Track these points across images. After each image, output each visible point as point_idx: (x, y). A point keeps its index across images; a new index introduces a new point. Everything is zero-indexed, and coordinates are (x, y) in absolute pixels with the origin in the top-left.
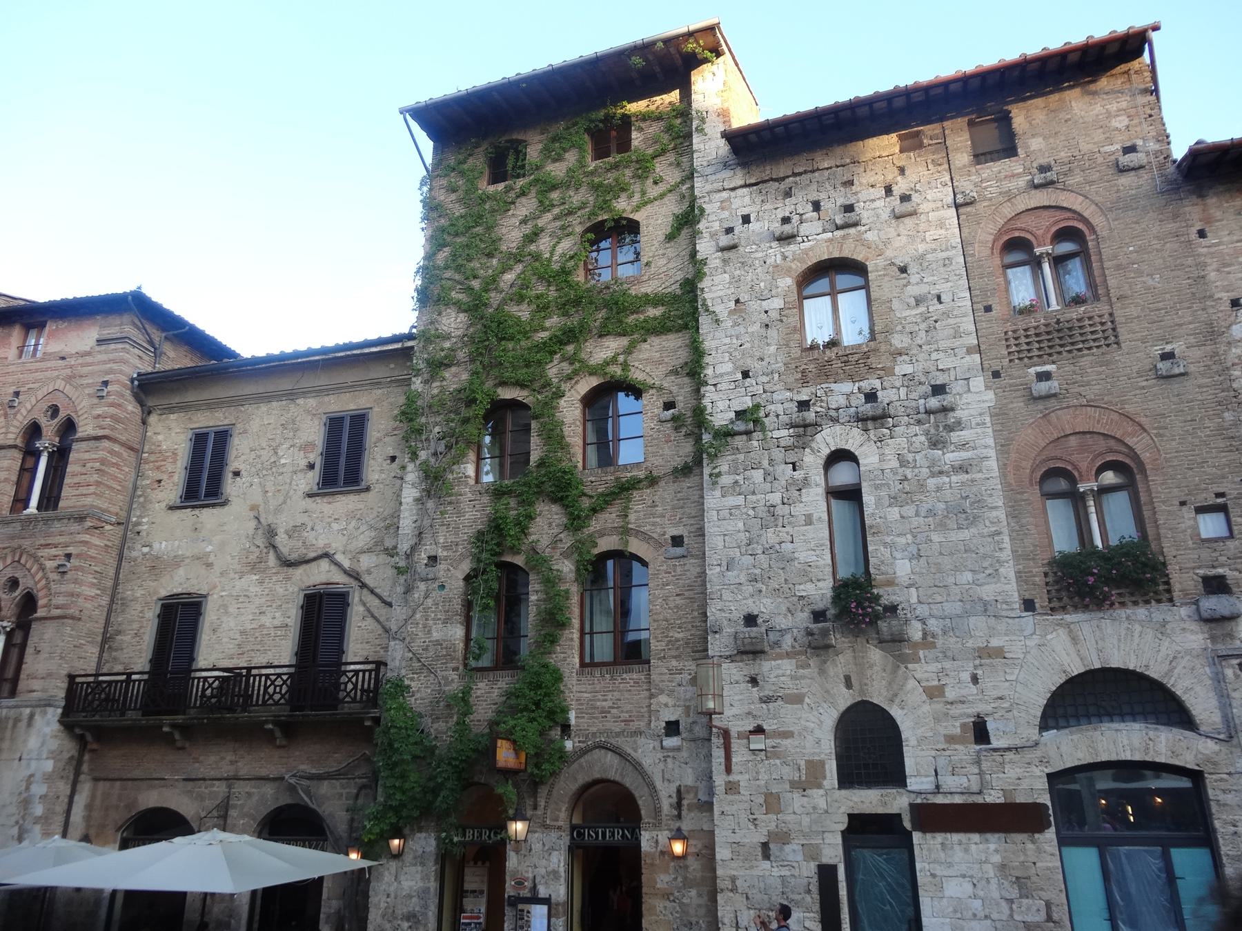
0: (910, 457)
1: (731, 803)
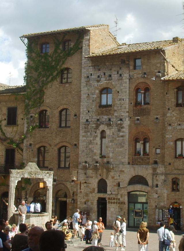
1: (80, 195)
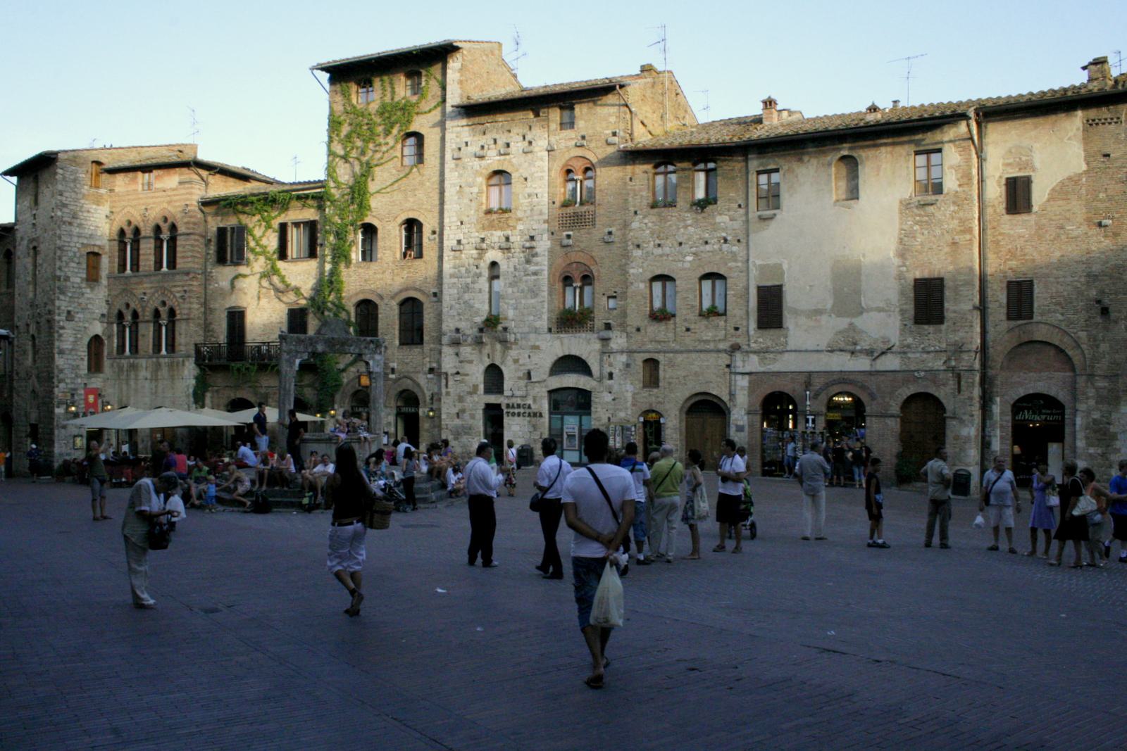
0: (518, 267)
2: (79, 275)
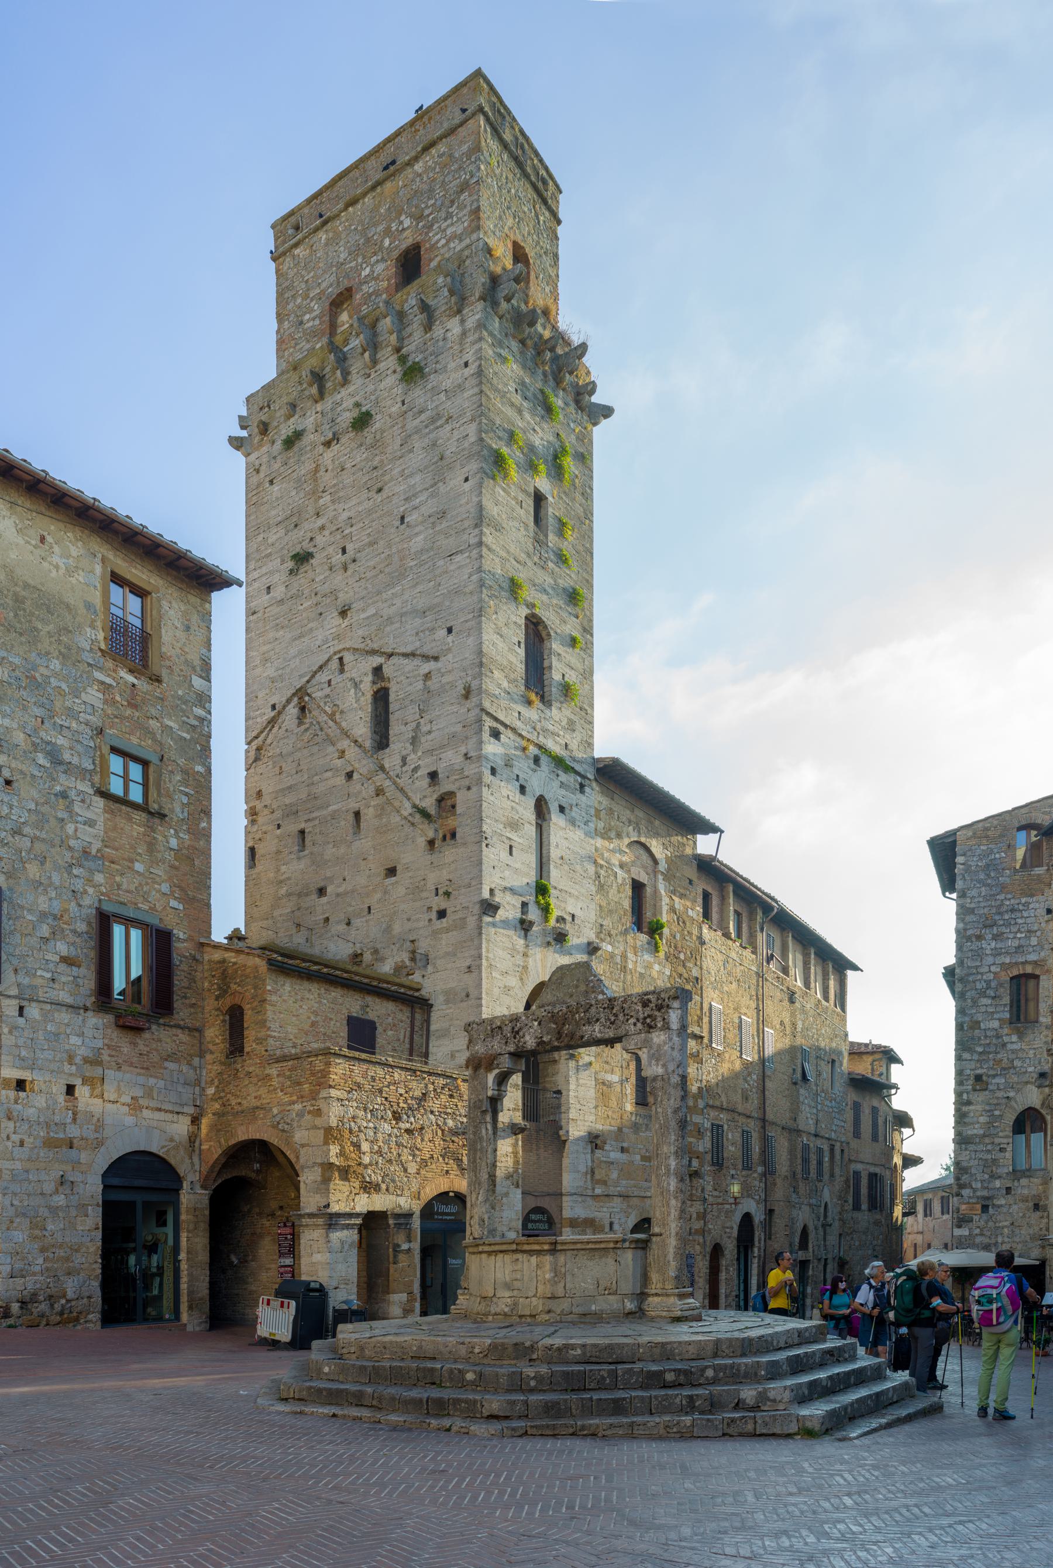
2: (995, 1016)
